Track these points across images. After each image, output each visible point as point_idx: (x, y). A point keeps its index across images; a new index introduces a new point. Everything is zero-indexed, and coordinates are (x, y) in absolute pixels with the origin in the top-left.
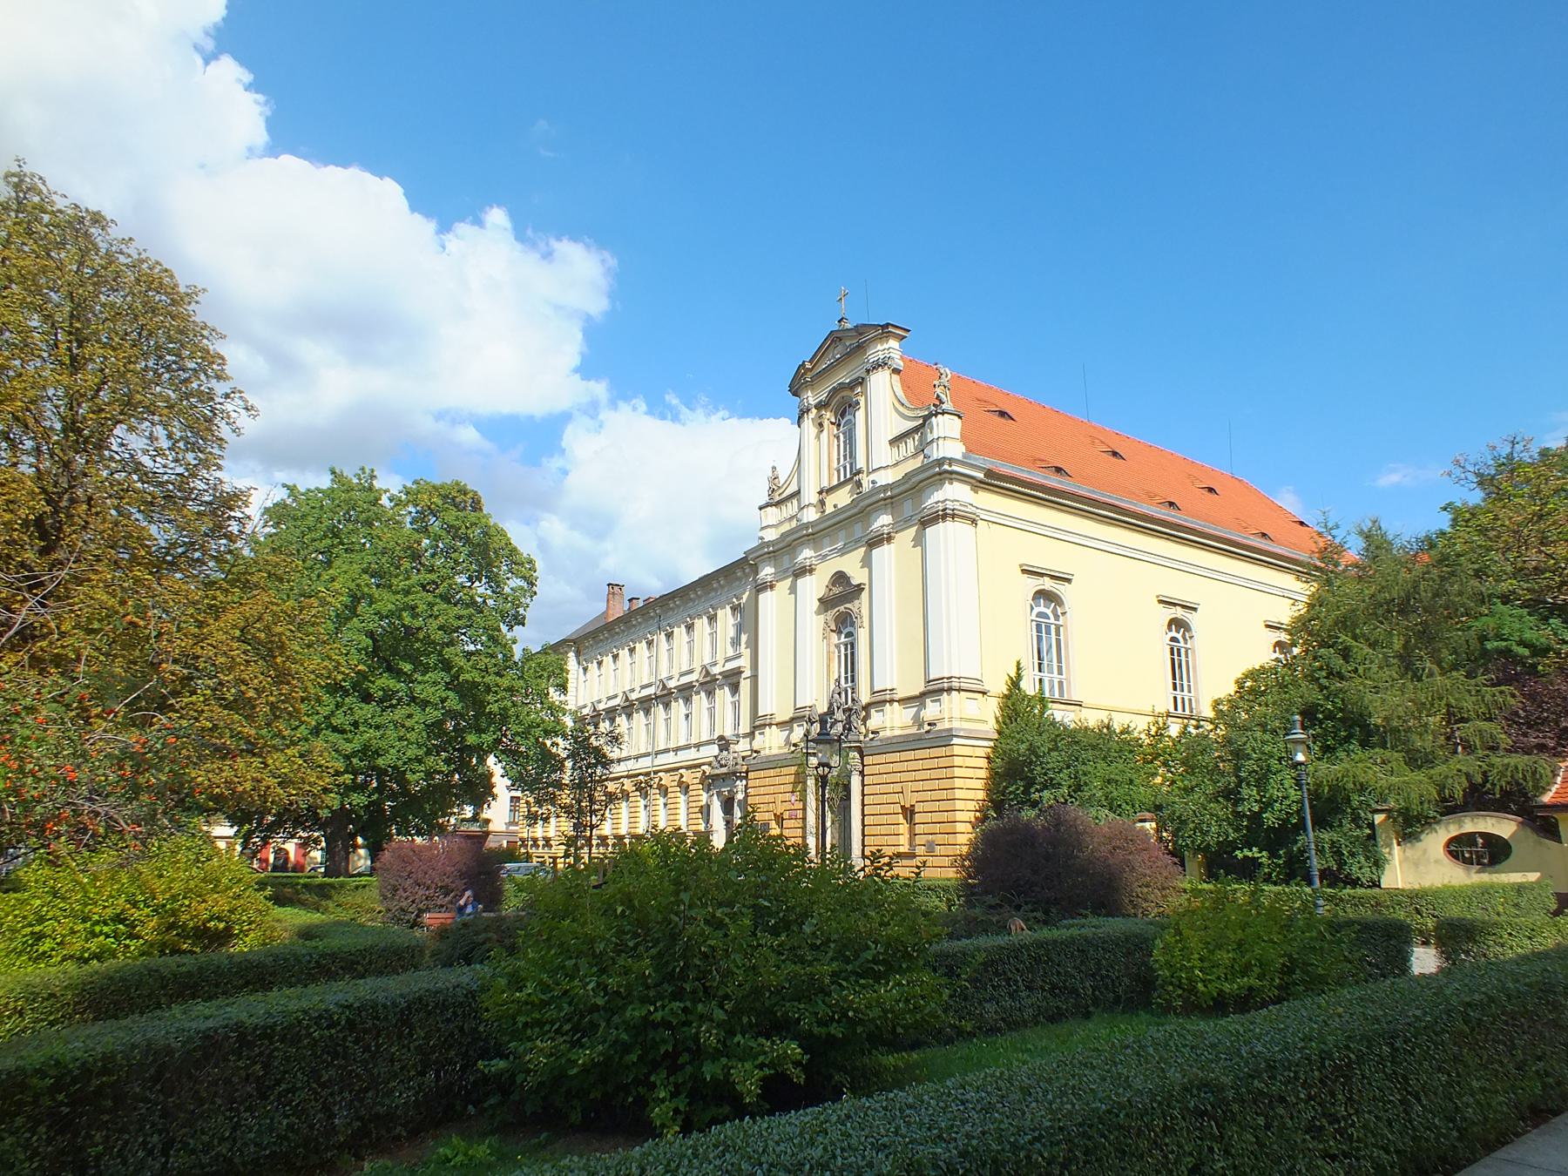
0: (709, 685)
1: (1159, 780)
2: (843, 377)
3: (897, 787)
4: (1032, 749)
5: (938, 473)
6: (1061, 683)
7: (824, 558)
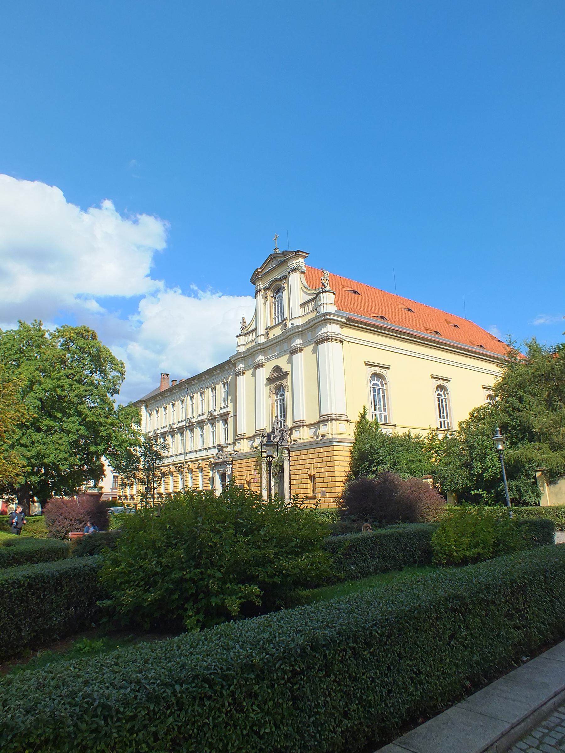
0: (212, 420)
1: (433, 459)
2: (277, 275)
3: (307, 466)
4: (372, 447)
5: (325, 319)
6: (385, 416)
7: (269, 359)
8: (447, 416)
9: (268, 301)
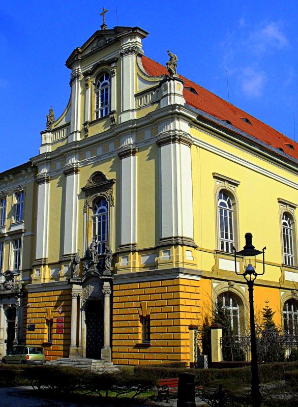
2: (106, 56)
3: (138, 304)
5: (172, 114)
7: (85, 164)
8: (291, 250)
9: (89, 89)
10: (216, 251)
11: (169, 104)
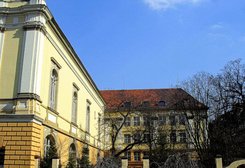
10: (48, 107)
11: (37, 3)
